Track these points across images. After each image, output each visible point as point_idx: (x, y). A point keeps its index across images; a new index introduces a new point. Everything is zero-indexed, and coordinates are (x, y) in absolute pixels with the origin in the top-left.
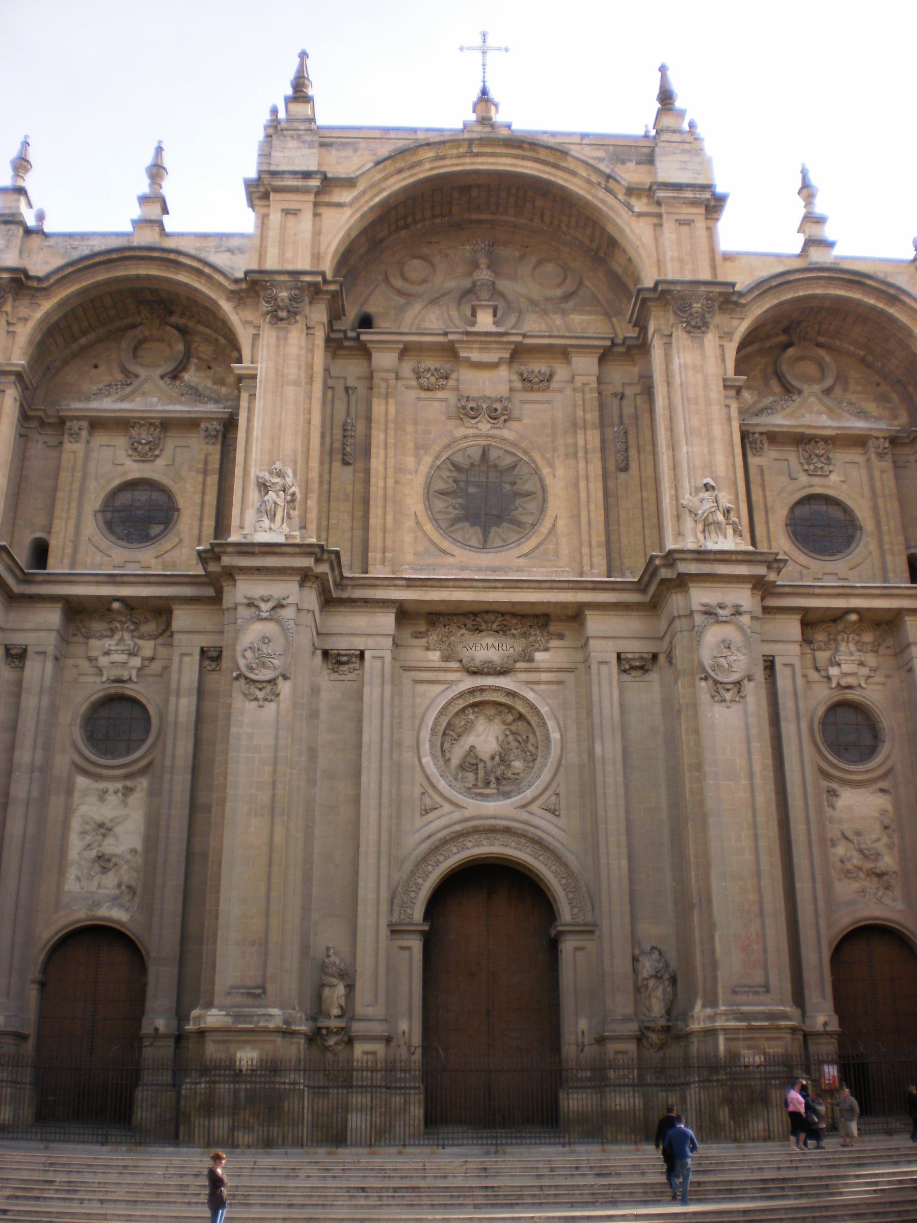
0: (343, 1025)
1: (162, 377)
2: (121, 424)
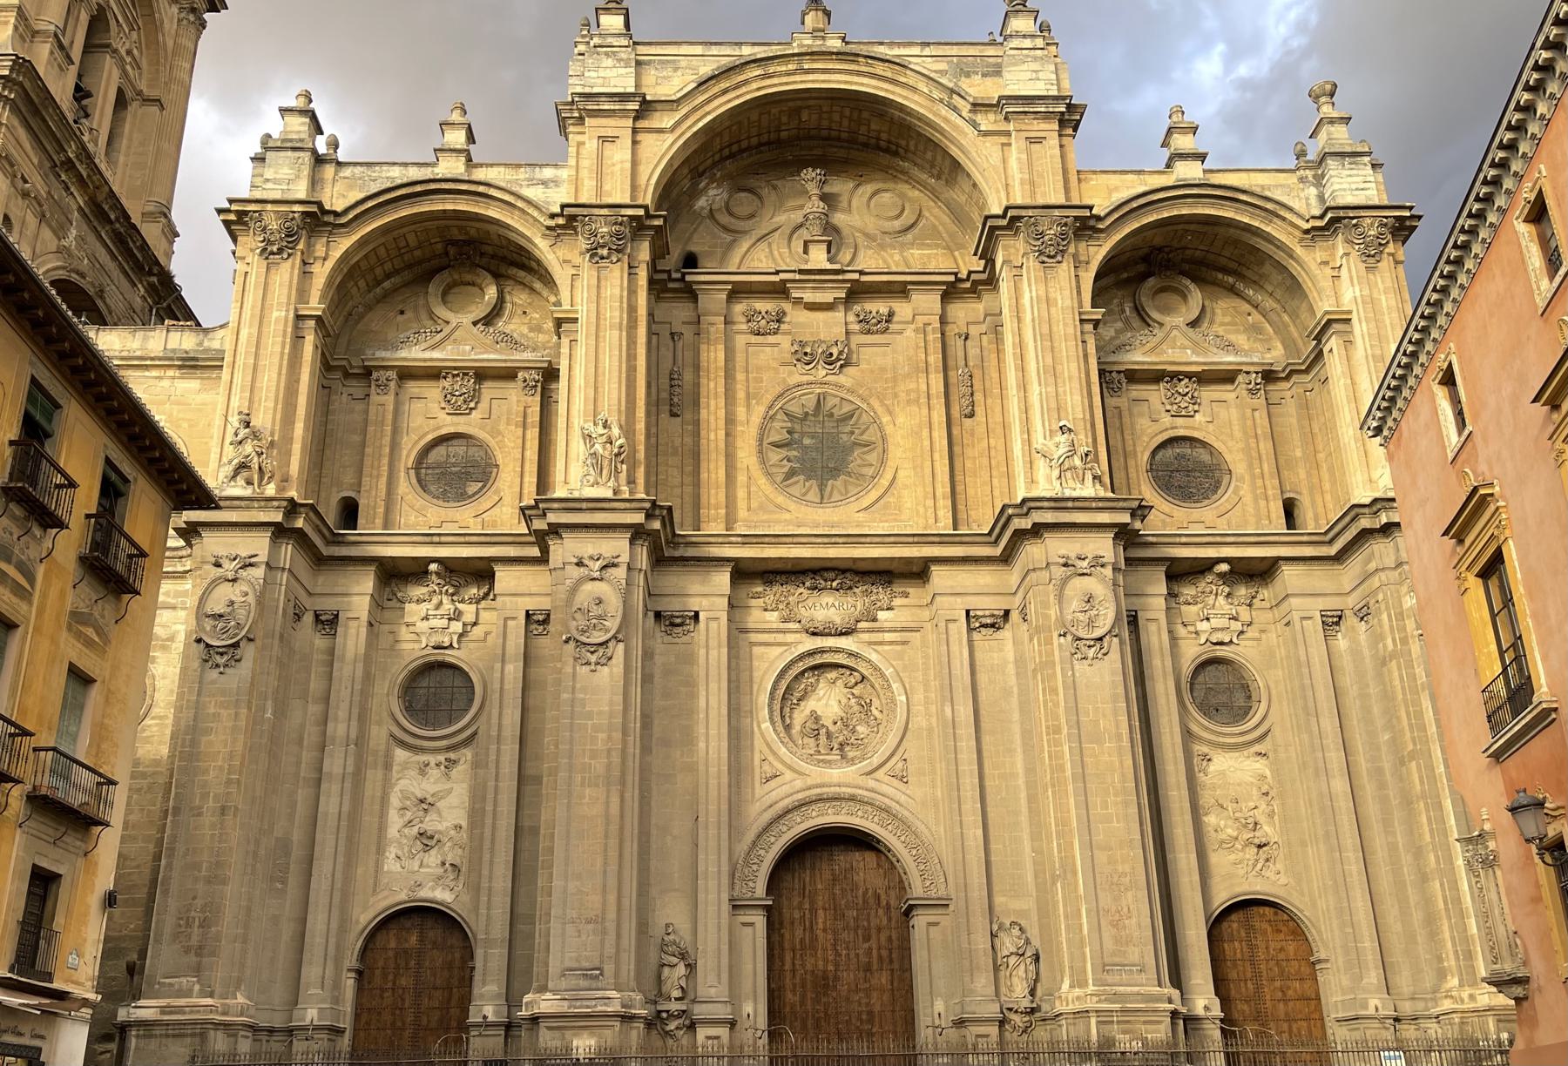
1: (475, 324)
2: (433, 374)
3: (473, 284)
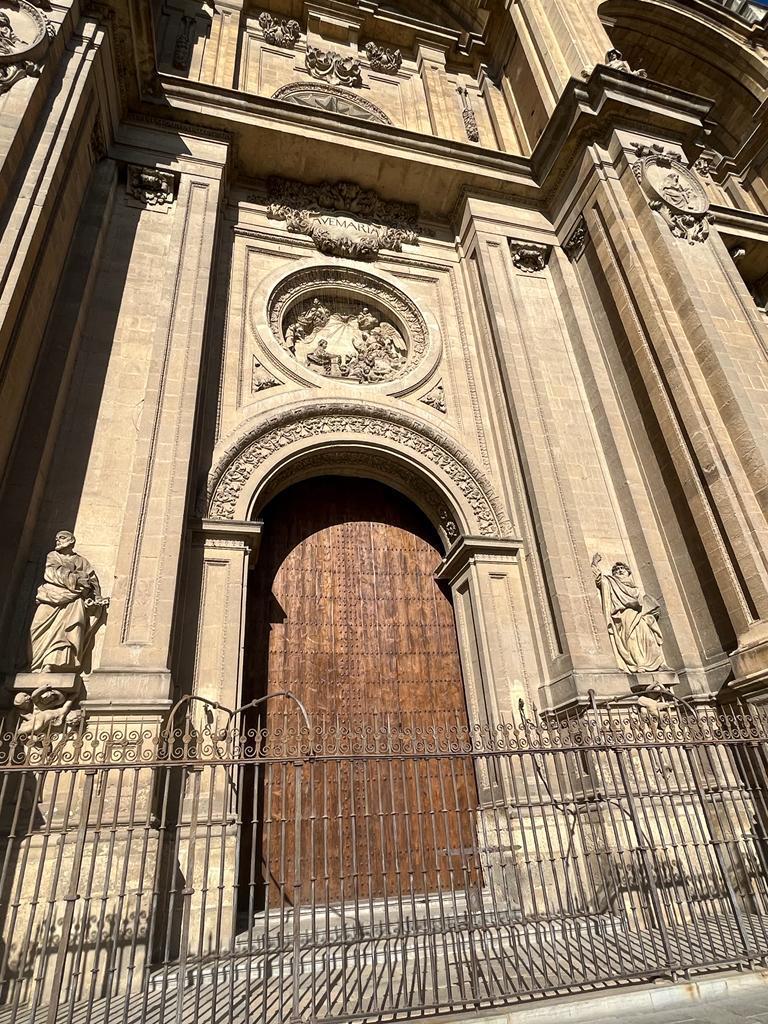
0: (67, 681)
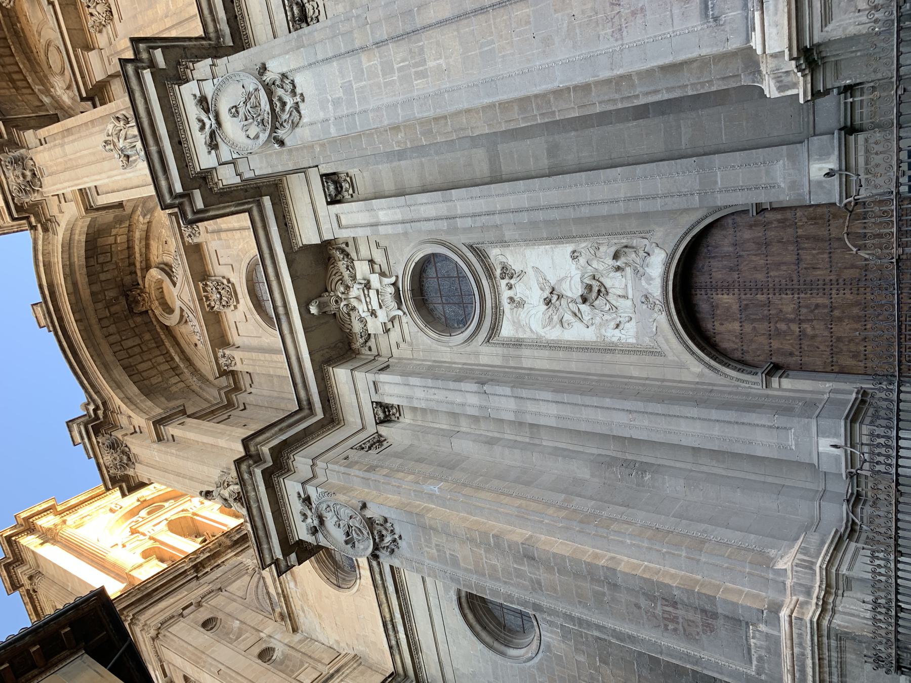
1: (174, 284)
3: (160, 289)
